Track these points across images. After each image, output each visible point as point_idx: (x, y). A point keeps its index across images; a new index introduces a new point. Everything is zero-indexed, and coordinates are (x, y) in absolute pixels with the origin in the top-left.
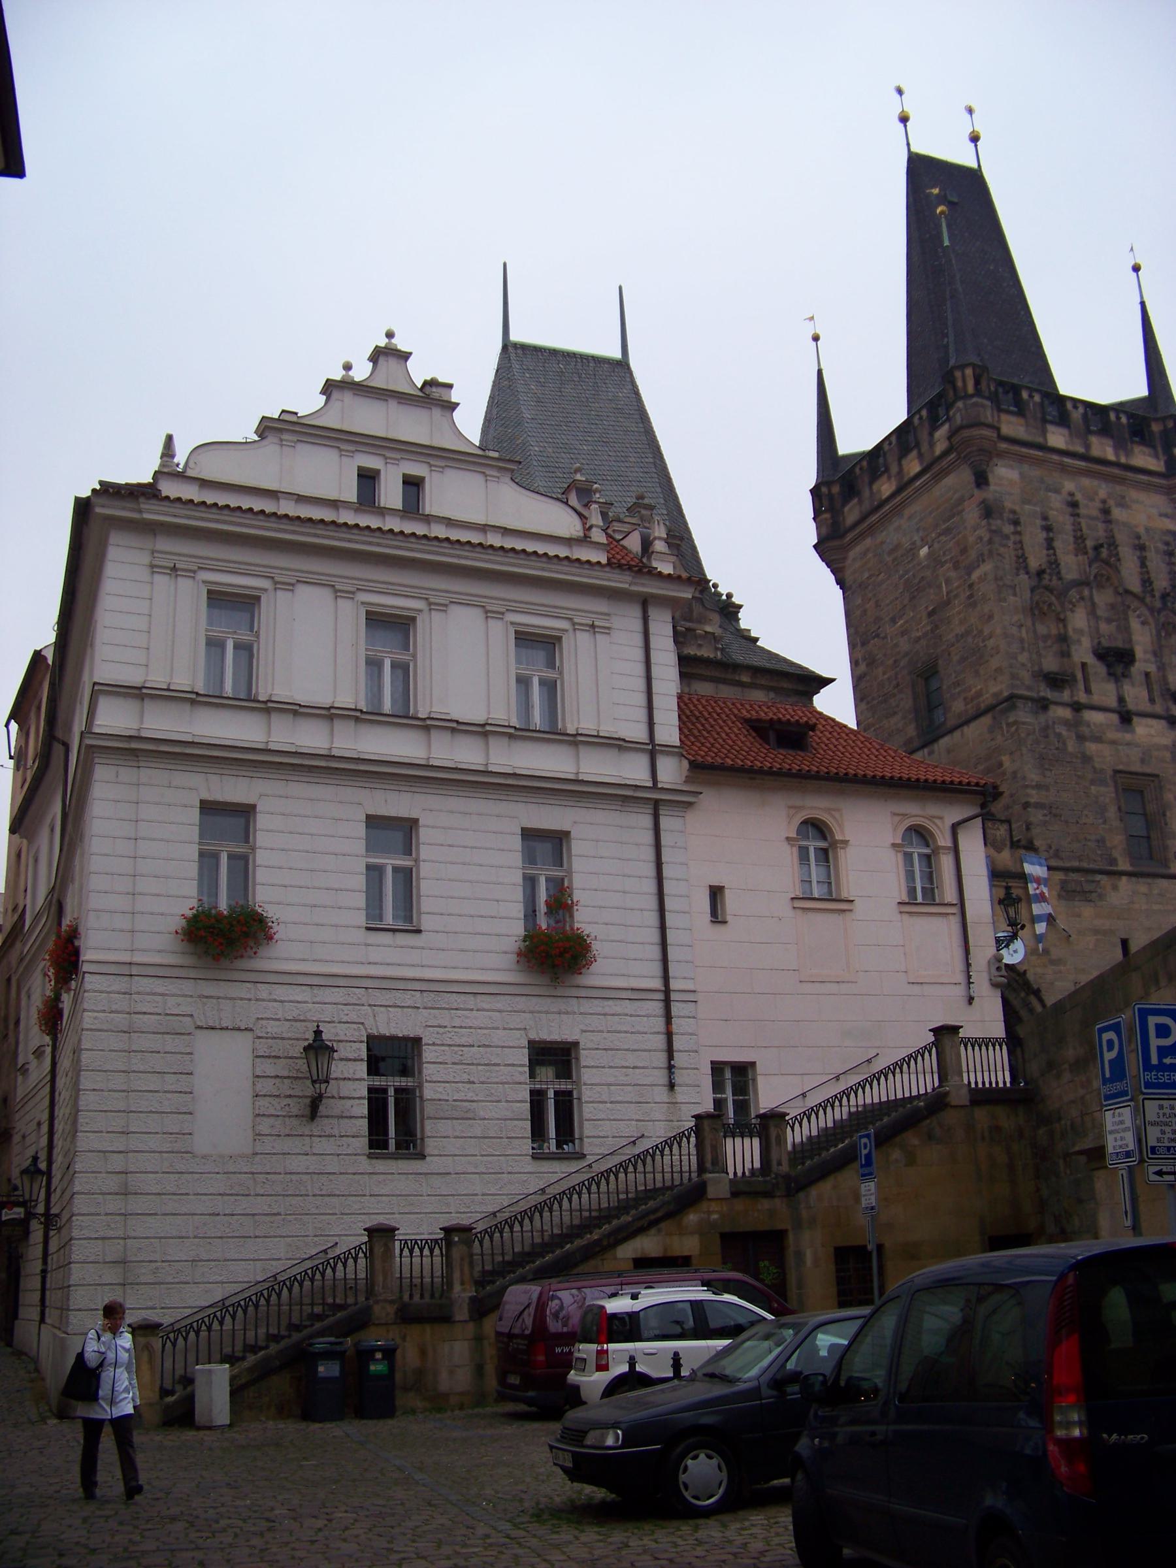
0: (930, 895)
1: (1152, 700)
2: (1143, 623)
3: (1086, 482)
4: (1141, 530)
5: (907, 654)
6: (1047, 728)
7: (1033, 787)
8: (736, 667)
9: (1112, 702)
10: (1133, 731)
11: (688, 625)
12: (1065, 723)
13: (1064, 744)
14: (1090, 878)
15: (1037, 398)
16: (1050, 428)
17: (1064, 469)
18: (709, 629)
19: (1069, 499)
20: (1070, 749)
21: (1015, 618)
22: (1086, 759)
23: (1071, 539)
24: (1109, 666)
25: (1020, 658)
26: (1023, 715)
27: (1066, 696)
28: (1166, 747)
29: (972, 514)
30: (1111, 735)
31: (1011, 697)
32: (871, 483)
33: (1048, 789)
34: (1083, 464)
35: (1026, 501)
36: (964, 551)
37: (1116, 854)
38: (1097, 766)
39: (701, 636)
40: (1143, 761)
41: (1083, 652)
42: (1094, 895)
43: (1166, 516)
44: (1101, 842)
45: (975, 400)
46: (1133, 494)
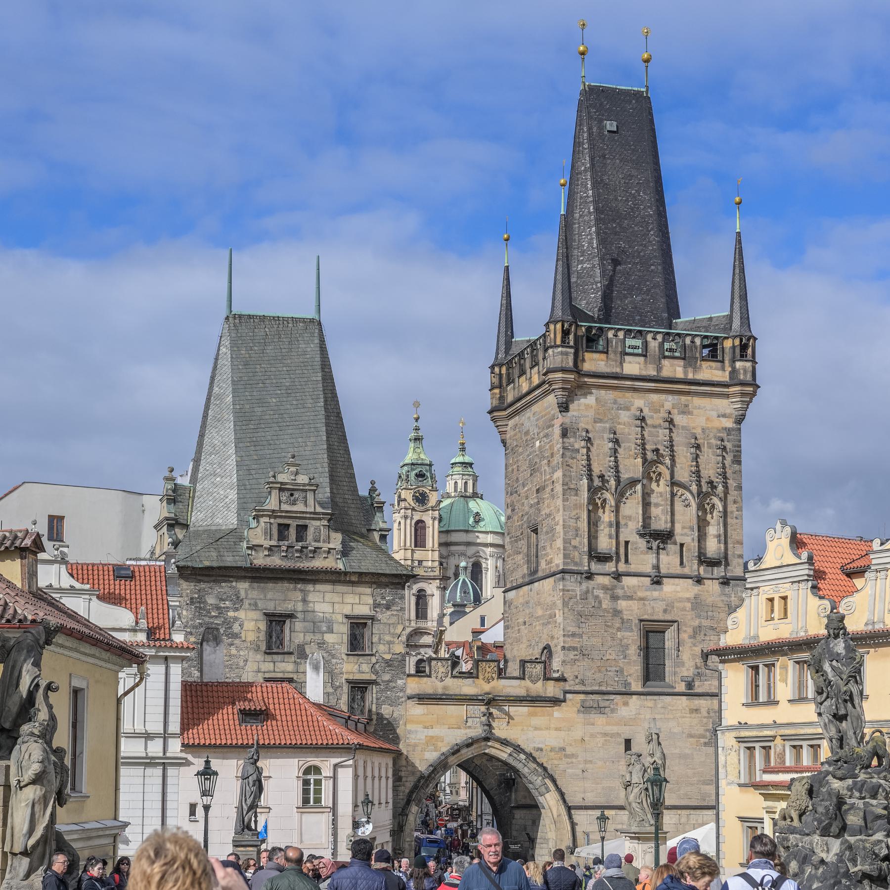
0: (318, 800)
1: (682, 563)
2: (686, 506)
3: (655, 397)
4: (698, 431)
5: (527, 513)
6: (587, 592)
7: (568, 636)
8: (346, 573)
9: (648, 569)
10: (662, 589)
11: (317, 545)
12: (605, 588)
13: (600, 602)
14: (606, 697)
15: (621, 335)
16: (627, 358)
17: (635, 390)
18: (331, 546)
19: (638, 413)
20: (604, 606)
21: (574, 513)
22: (617, 613)
23: (633, 446)
24: (648, 542)
25: (574, 543)
26: (571, 583)
27: (610, 567)
28: (688, 599)
29: (557, 431)
30: (640, 594)
31: (563, 572)
32: (519, 377)
33: (581, 636)
34: (653, 385)
35: (595, 422)
36: (552, 455)
37: (630, 680)
38: (625, 617)
39: (324, 552)
40: (665, 611)
41: (630, 532)
43: (724, 416)
44: (620, 672)
45: (560, 349)
46: (697, 401)
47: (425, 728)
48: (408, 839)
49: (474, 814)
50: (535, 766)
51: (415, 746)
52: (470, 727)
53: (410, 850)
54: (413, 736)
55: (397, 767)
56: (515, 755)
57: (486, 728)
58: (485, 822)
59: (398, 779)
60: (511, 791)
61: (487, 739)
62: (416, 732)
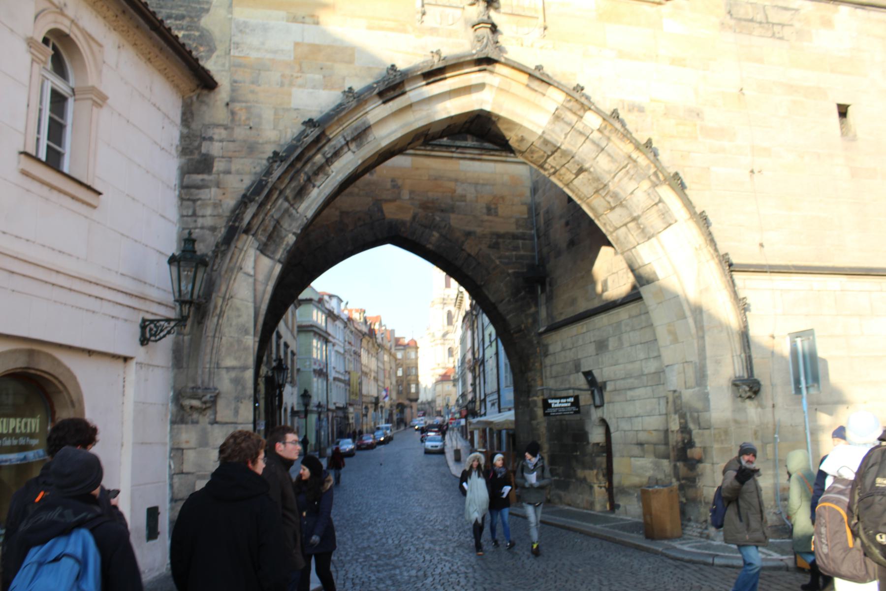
42: (787, 31)
47: (295, 20)
48: (229, 362)
49: (478, 403)
50: (629, 148)
51: (260, 68)
52: (433, 31)
53: (238, 399)
54: (253, 40)
55: (195, 126)
56: (570, 117)
57: (485, 31)
58: (489, 405)
59: (196, 163)
60: (537, 305)
61: (485, 62)
62: (265, 29)
